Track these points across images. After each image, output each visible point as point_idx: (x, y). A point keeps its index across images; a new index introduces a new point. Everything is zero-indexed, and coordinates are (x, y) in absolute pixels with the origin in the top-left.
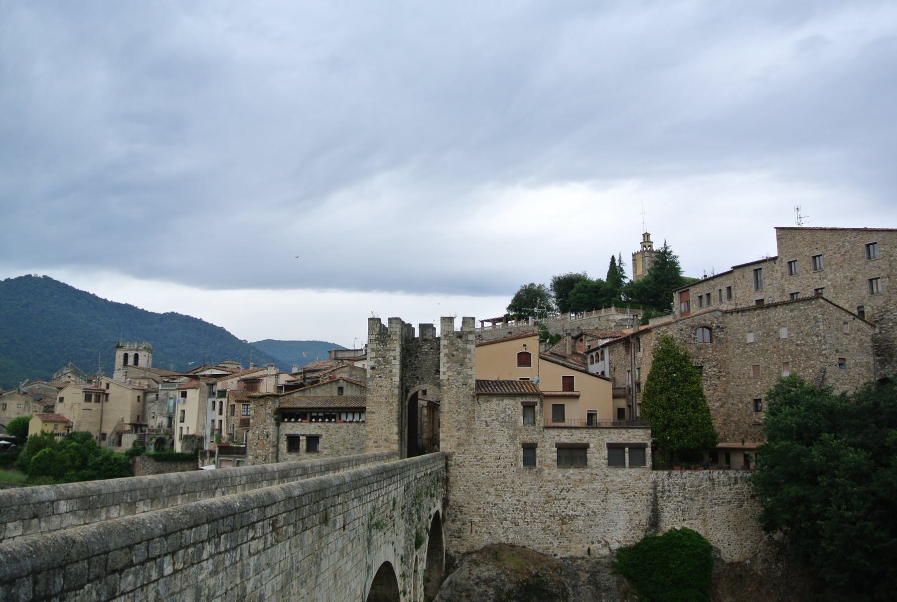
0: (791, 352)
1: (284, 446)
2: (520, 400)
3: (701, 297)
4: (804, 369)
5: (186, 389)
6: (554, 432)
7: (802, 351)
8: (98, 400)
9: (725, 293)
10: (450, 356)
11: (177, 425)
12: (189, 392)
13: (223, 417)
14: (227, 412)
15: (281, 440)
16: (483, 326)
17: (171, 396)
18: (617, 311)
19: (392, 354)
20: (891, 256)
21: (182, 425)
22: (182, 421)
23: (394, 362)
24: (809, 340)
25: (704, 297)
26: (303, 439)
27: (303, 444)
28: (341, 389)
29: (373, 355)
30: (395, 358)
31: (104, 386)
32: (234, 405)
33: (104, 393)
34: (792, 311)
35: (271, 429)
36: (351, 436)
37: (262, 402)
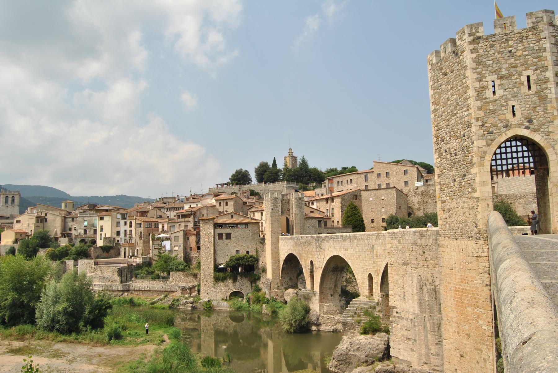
0: (385, 204)
1: (217, 237)
2: (317, 219)
3: (338, 182)
4: (389, 210)
5: (104, 216)
6: (327, 230)
7: (389, 204)
8: (41, 222)
9: (349, 181)
10: (297, 205)
11: (99, 232)
12: (105, 218)
13: (133, 228)
14: (135, 226)
15: (216, 235)
16: (217, 187)
17: (86, 219)
18: (287, 183)
19: (279, 204)
20: (412, 174)
21: (101, 233)
22: (102, 230)
23: (279, 207)
24: (391, 200)
25: (340, 182)
26: (224, 235)
27: (224, 237)
28: (232, 217)
29: (272, 205)
30: (279, 206)
31: (43, 215)
32: (141, 223)
33: (44, 218)
34: (385, 191)
35: (212, 231)
36: (243, 233)
37: (207, 221)
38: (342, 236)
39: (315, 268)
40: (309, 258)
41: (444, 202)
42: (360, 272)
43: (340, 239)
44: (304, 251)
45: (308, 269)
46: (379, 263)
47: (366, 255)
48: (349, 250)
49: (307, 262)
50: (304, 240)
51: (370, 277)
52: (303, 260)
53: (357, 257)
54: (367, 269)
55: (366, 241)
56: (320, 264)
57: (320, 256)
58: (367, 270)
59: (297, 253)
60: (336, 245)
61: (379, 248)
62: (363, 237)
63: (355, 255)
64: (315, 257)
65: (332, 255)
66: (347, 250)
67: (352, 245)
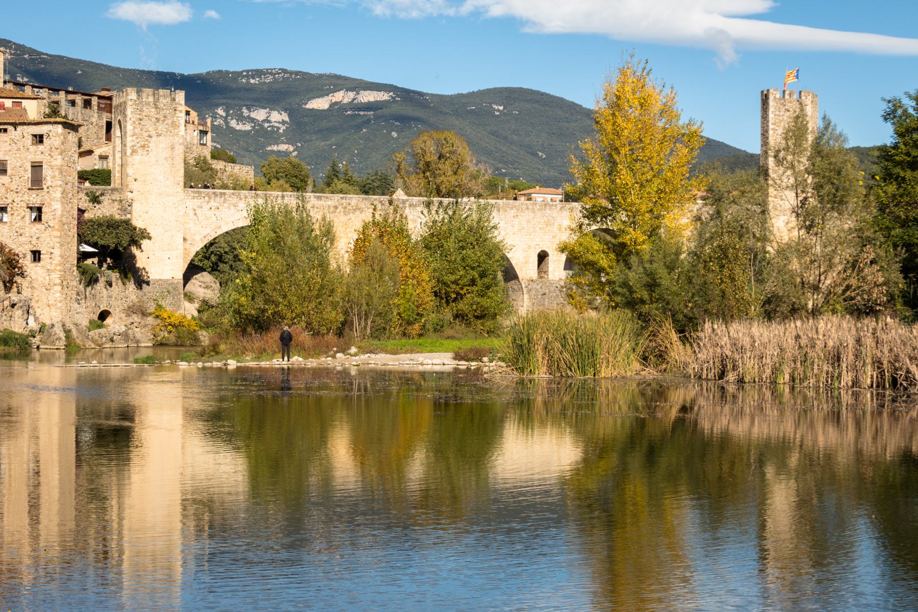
47: (537, 229)
55: (539, 214)
58: (537, 247)
62: (530, 207)
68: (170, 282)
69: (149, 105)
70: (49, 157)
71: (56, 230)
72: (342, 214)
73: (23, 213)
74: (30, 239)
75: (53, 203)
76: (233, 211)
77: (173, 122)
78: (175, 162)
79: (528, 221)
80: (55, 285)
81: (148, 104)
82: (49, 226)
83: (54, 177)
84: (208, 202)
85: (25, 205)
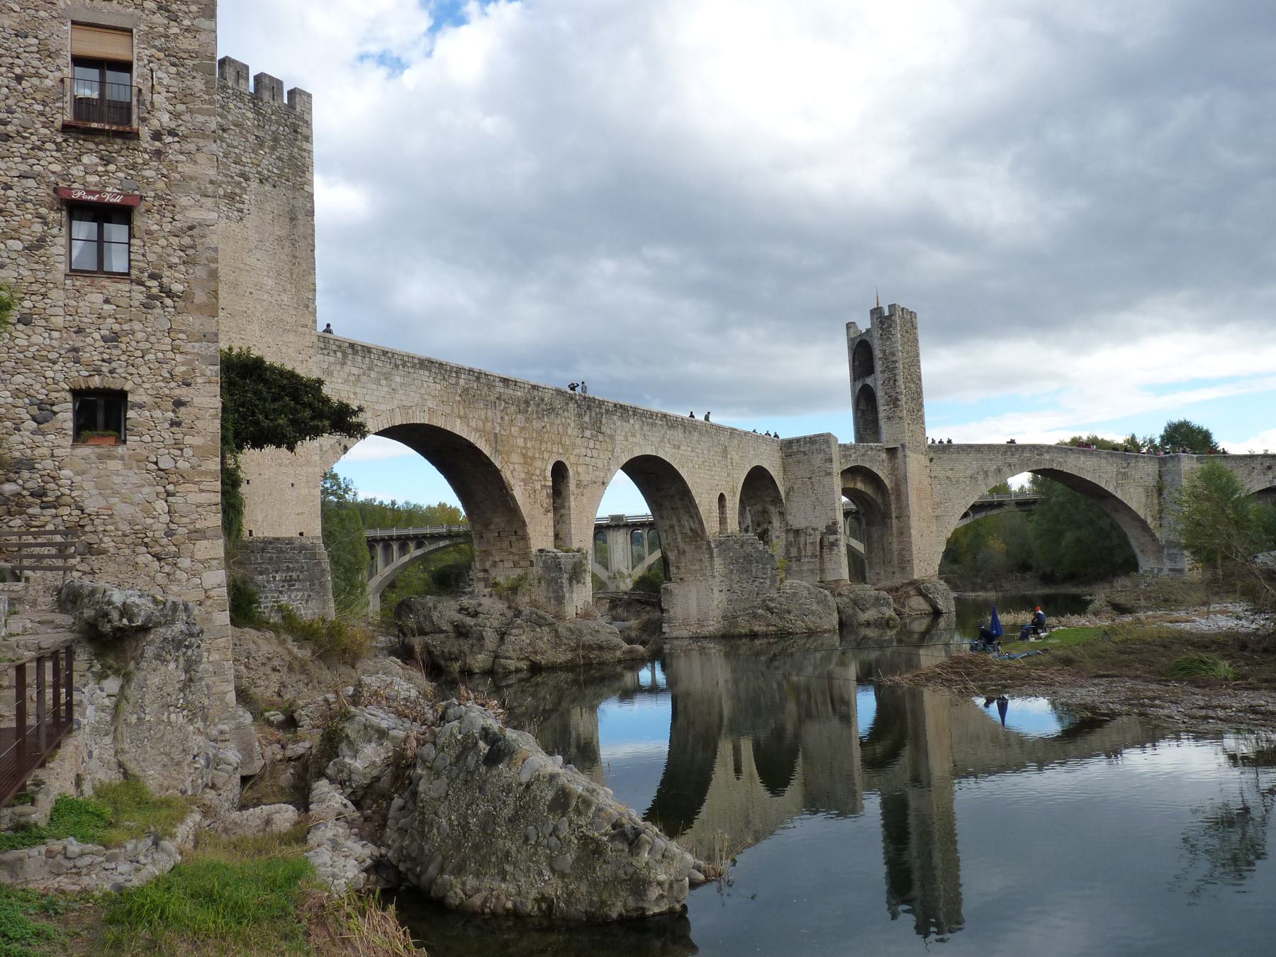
38: (665, 416)
39: (578, 485)
40: (546, 455)
41: (909, 424)
42: (705, 491)
43: (660, 422)
44: (522, 429)
45: (544, 487)
46: (735, 476)
47: (716, 462)
48: (682, 448)
49: (538, 464)
50: (519, 393)
51: (722, 497)
52: (515, 458)
53: (700, 463)
54: (717, 485)
56: (597, 473)
57: (594, 451)
59: (476, 430)
60: (649, 434)
61: (734, 453)
63: (696, 459)
64: (575, 453)
65: (637, 453)
66: (679, 448)
67: (688, 440)
68: (297, 543)
69: (242, 100)
70: (159, 19)
71: (200, 309)
72: (535, 416)
73: (38, 228)
74: (78, 341)
75: (184, 201)
76: (386, 389)
77: (291, 157)
78: (298, 254)
79: (709, 451)
80: (197, 535)
81: (239, 96)
82: (170, 294)
83: (185, 96)
84: (345, 363)
85: (44, 192)
